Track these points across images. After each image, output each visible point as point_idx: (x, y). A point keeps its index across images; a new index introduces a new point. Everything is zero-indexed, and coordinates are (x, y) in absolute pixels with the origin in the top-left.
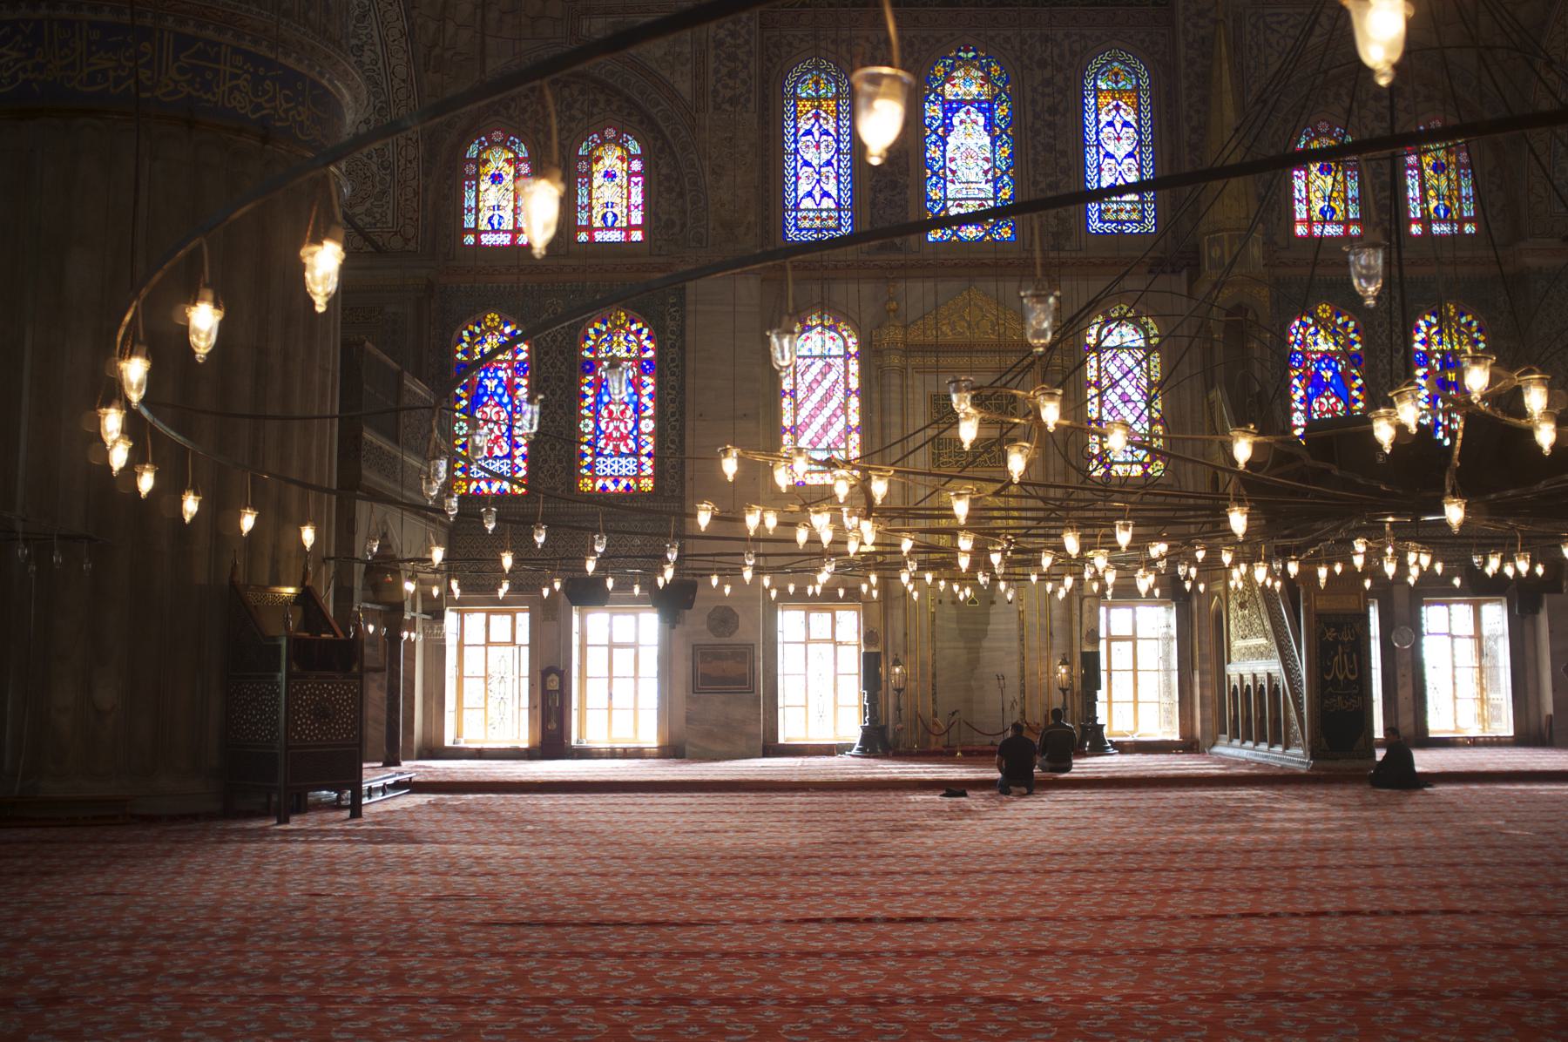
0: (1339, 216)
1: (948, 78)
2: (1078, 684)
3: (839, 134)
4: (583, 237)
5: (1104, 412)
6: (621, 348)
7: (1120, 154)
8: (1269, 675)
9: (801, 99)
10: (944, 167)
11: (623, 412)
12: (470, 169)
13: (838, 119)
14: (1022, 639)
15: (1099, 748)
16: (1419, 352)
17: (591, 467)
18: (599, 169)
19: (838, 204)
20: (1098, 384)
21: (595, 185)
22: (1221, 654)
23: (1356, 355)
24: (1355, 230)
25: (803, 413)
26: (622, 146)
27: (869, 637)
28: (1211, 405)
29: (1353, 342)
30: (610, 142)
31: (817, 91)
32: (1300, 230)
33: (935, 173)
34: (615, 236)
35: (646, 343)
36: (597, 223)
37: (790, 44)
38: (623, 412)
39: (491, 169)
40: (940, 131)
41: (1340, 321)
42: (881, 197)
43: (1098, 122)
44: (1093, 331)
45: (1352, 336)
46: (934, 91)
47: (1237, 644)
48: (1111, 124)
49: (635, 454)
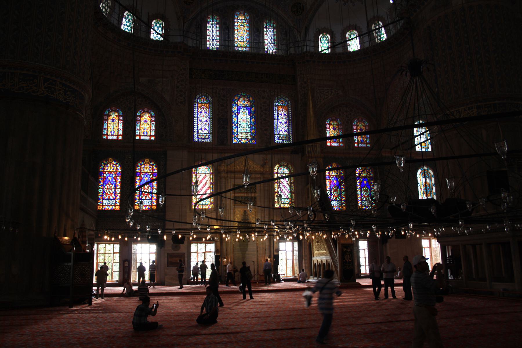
1: (238, 100)
2: (272, 264)
4: (137, 138)
6: (146, 169)
8: (327, 260)
11: (148, 187)
12: (106, 117)
14: (258, 251)
15: (279, 281)
21: (142, 123)
22: (311, 255)
24: (341, 144)
26: (149, 113)
27: (217, 251)
30: (146, 112)
34: (148, 138)
35: (155, 168)
36: (142, 134)
38: (148, 187)
43: (278, 114)
46: (235, 103)
47: (316, 252)
48: (281, 114)
49: (151, 199)
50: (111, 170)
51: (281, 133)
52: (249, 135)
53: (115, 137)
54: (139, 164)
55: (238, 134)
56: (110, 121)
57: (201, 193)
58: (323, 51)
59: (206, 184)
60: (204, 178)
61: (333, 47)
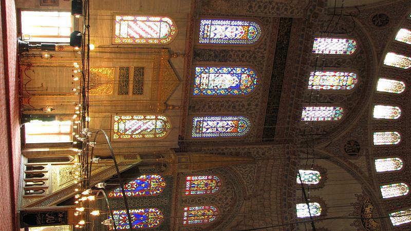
10: (220, 73)
14: (60, 95)
16: (149, 210)
19: (211, 39)
20: (145, 119)
28: (134, 157)
29: (153, 192)
31: (250, 33)
33: (218, 70)
37: (267, 25)
40: (232, 72)
42: (212, 53)
43: (229, 121)
44: (161, 118)
45: (155, 192)
48: (228, 124)
52: (204, 86)
55: (206, 73)
58: (299, 176)
61: (303, 186)
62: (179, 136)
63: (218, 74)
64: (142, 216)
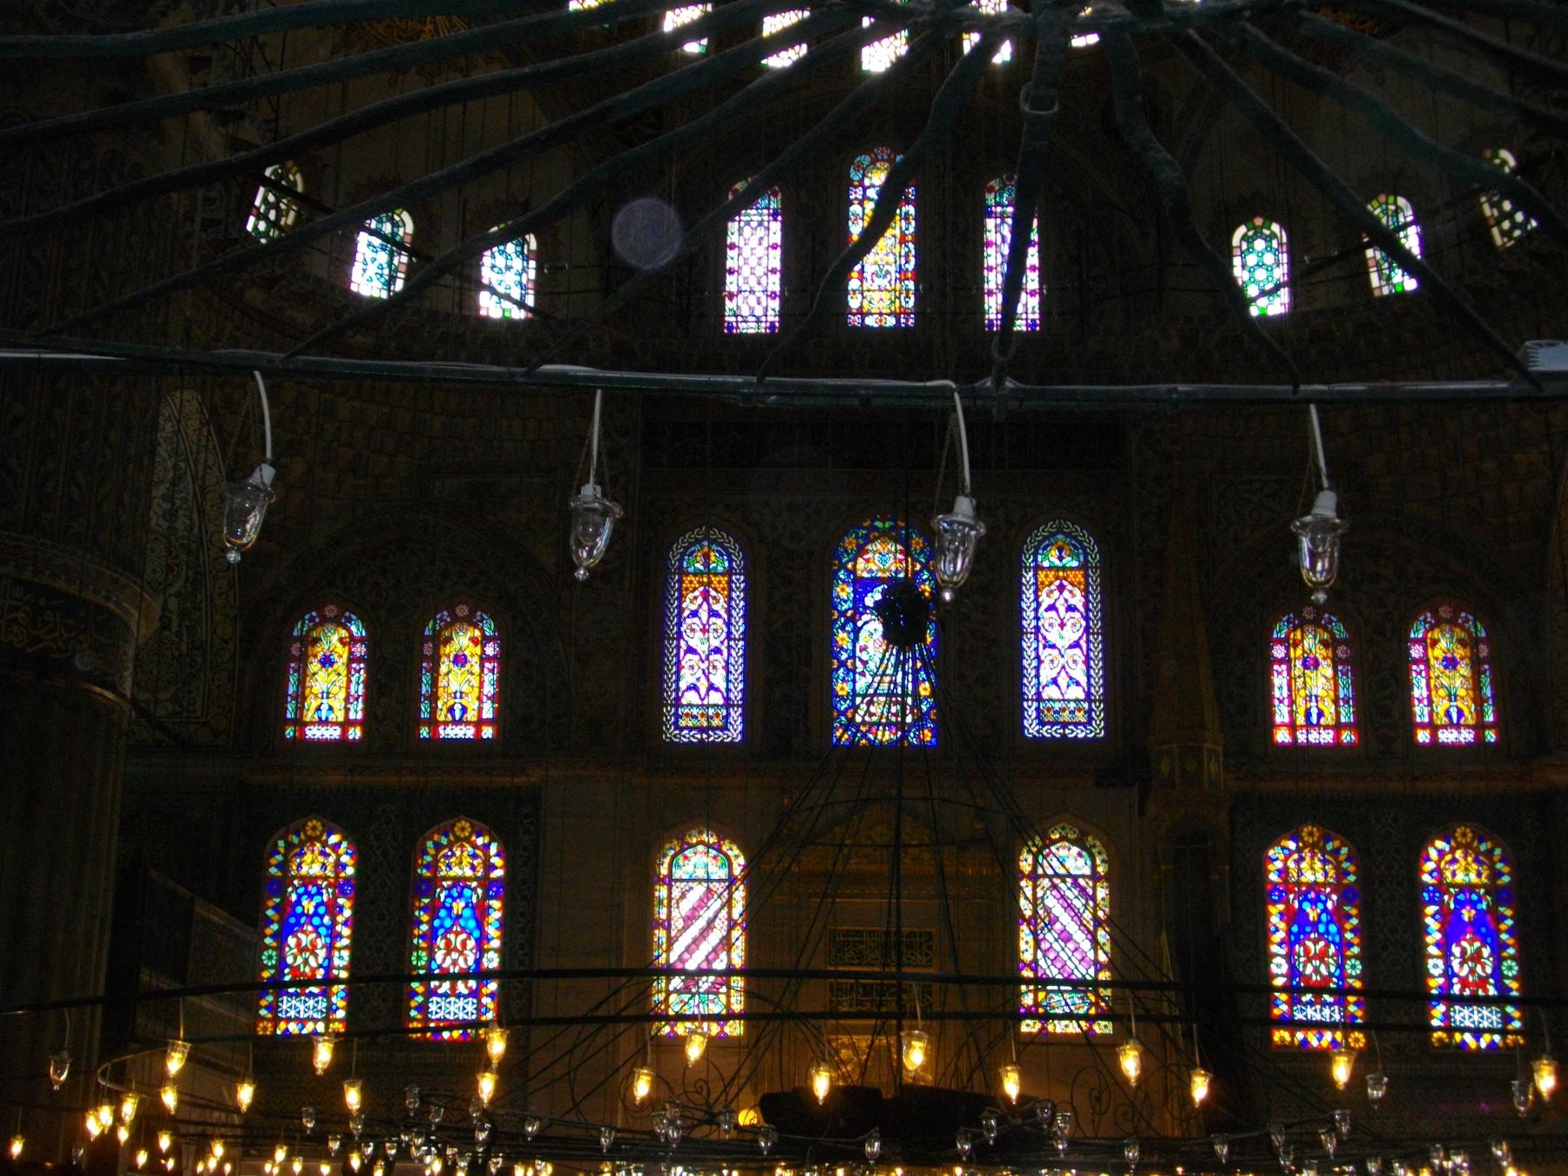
0: (1328, 719)
1: (861, 551)
3: (730, 615)
5: (1040, 954)
6: (467, 861)
7: (1062, 644)
9: (688, 574)
10: (853, 656)
11: (464, 944)
12: (295, 649)
13: (730, 599)
17: (423, 1008)
18: (450, 649)
19: (727, 699)
23: (1350, 887)
25: (678, 948)
26: (475, 626)
29: (1347, 873)
31: (706, 564)
32: (1282, 736)
34: (469, 732)
36: (441, 718)
38: (464, 944)
39: (320, 650)
41: (1329, 847)
46: (843, 566)
48: (1052, 608)
49: (475, 994)
50: (316, 870)
51: (1050, 692)
53: (333, 733)
54: (430, 844)
56: (314, 666)
57: (691, 965)
59: (710, 925)
60: (703, 903)
62: (1097, 785)
63: (858, 664)
64: (1457, 913)
